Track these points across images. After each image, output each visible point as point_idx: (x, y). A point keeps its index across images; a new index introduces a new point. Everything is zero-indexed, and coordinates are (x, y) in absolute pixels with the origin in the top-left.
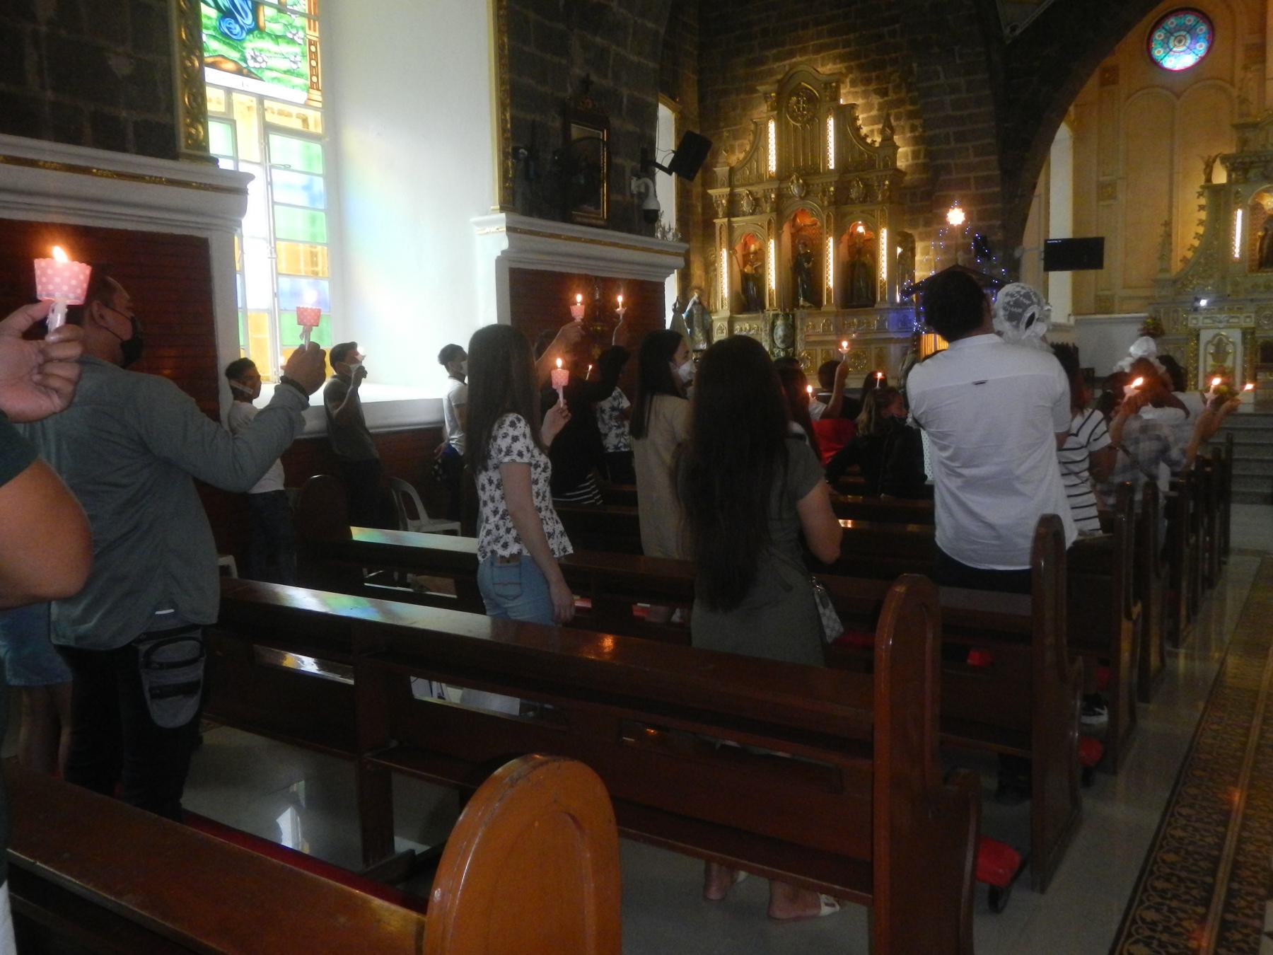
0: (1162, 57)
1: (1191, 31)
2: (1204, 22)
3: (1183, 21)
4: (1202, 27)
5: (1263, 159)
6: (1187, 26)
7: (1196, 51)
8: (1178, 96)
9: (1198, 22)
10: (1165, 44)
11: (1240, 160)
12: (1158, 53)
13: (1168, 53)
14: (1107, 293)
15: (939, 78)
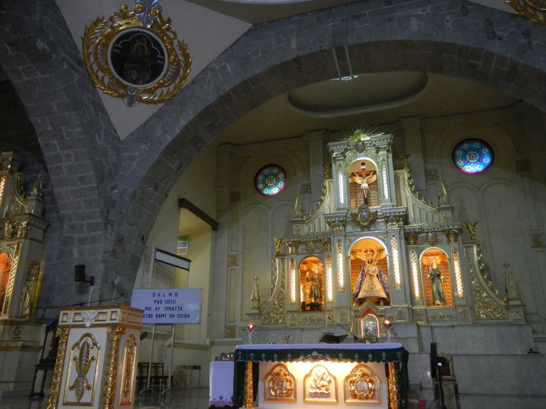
0: (262, 188)
1: (276, 176)
2: (282, 172)
3: (272, 171)
4: (281, 174)
5: (305, 240)
6: (274, 174)
7: (279, 187)
8: (270, 210)
9: (279, 172)
10: (264, 182)
11: (292, 240)
12: (260, 186)
13: (265, 187)
14: (232, 324)
15: (57, 150)
